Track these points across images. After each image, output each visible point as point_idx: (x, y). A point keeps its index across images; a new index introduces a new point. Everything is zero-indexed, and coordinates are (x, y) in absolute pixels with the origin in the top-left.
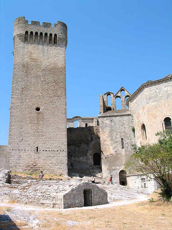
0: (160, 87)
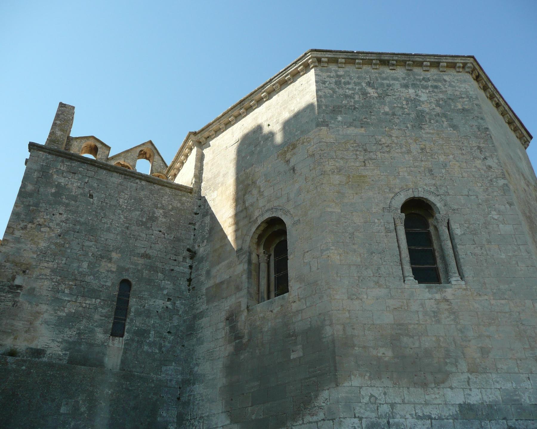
0: (385, 82)
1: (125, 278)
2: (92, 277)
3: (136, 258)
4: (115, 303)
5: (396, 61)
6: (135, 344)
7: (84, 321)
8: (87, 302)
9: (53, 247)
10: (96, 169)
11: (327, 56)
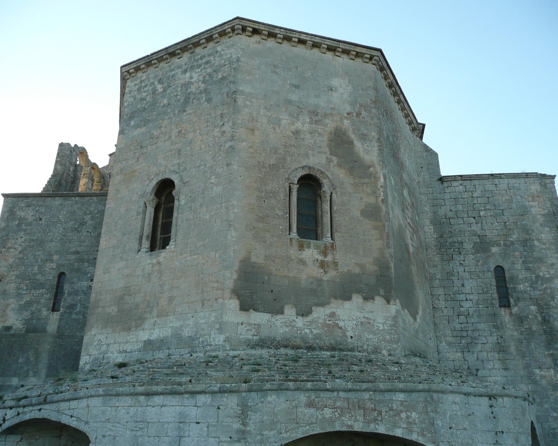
1: (62, 271)
2: (40, 275)
3: (69, 256)
4: (54, 290)
5: (180, 49)
6: (67, 315)
7: (35, 304)
8: (37, 292)
9: (17, 260)
10: (44, 198)
11: (132, 67)
